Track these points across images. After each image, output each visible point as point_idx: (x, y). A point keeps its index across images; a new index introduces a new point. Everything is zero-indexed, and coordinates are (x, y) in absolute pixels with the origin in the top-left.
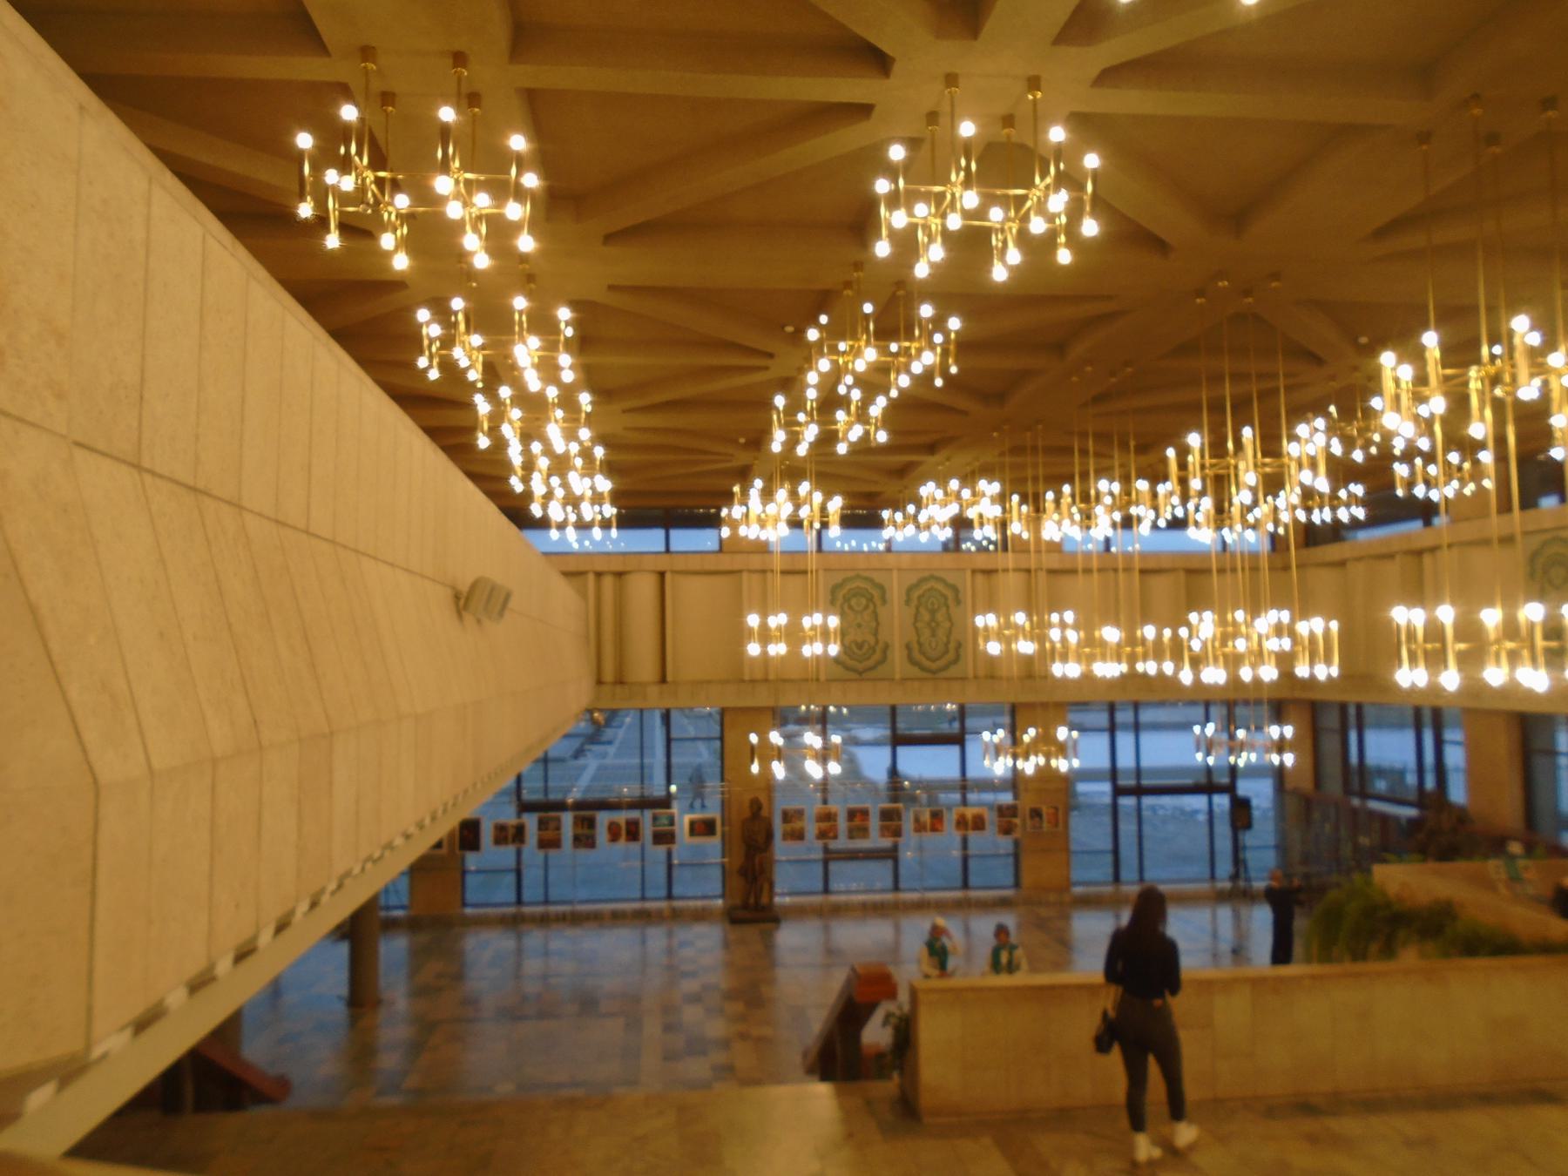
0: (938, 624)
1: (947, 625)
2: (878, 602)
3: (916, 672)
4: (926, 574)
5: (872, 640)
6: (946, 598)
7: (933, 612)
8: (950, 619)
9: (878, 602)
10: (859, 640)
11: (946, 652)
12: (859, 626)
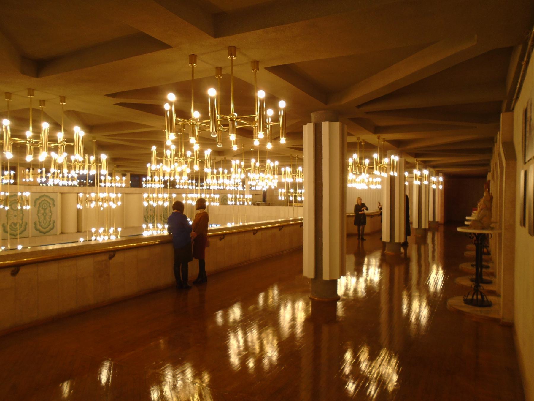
0: (46, 214)
1: (50, 214)
3: (38, 233)
4: (43, 194)
5: (21, 222)
6: (50, 203)
7: (45, 209)
8: (51, 212)
10: (15, 222)
11: (50, 225)
12: (15, 216)
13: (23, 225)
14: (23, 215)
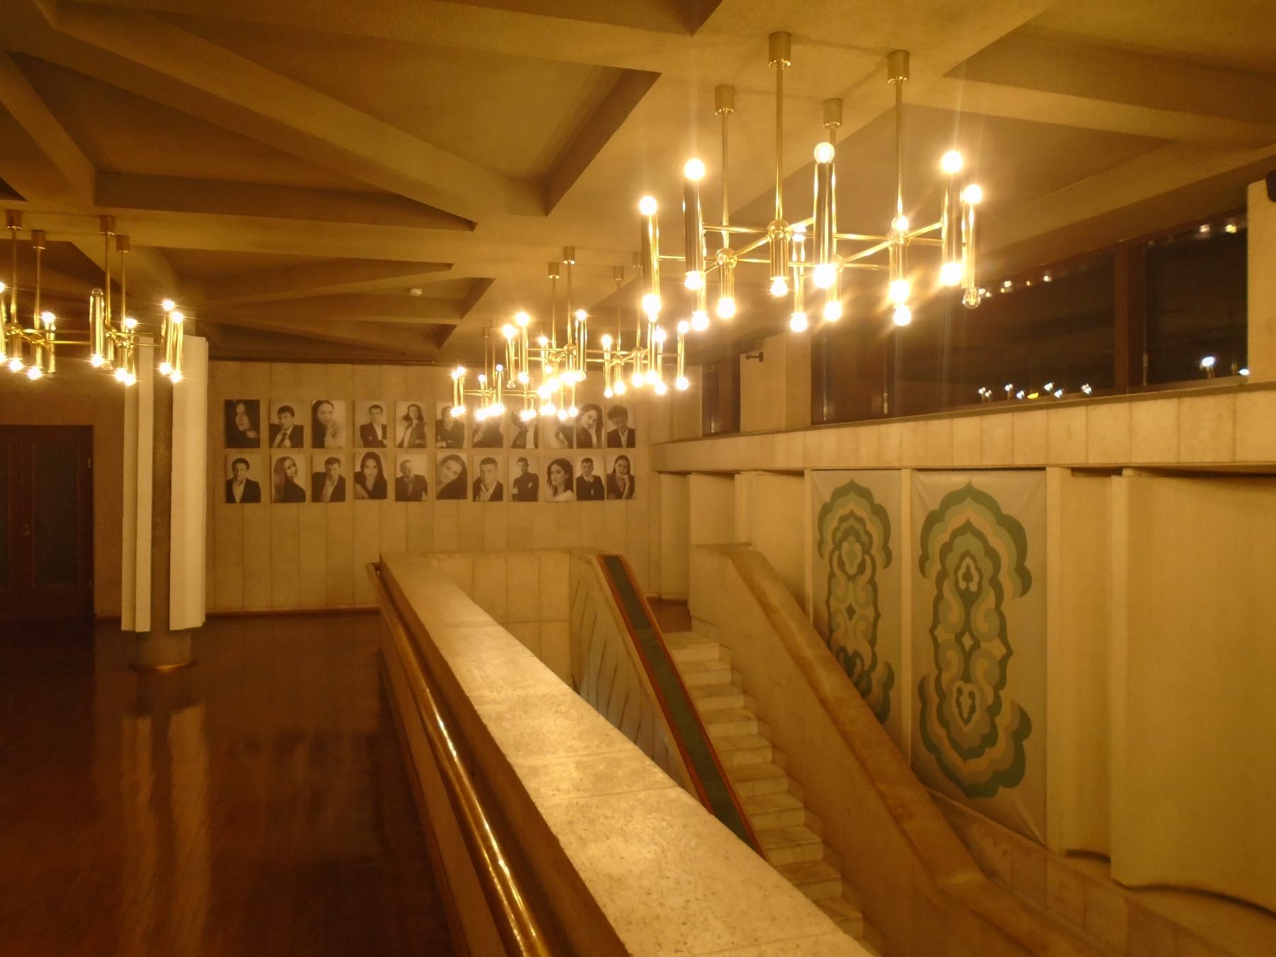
0: (976, 645)
1: (997, 649)
4: (959, 480)
7: (969, 600)
8: (1002, 635)
10: (850, 651)
11: (990, 738)
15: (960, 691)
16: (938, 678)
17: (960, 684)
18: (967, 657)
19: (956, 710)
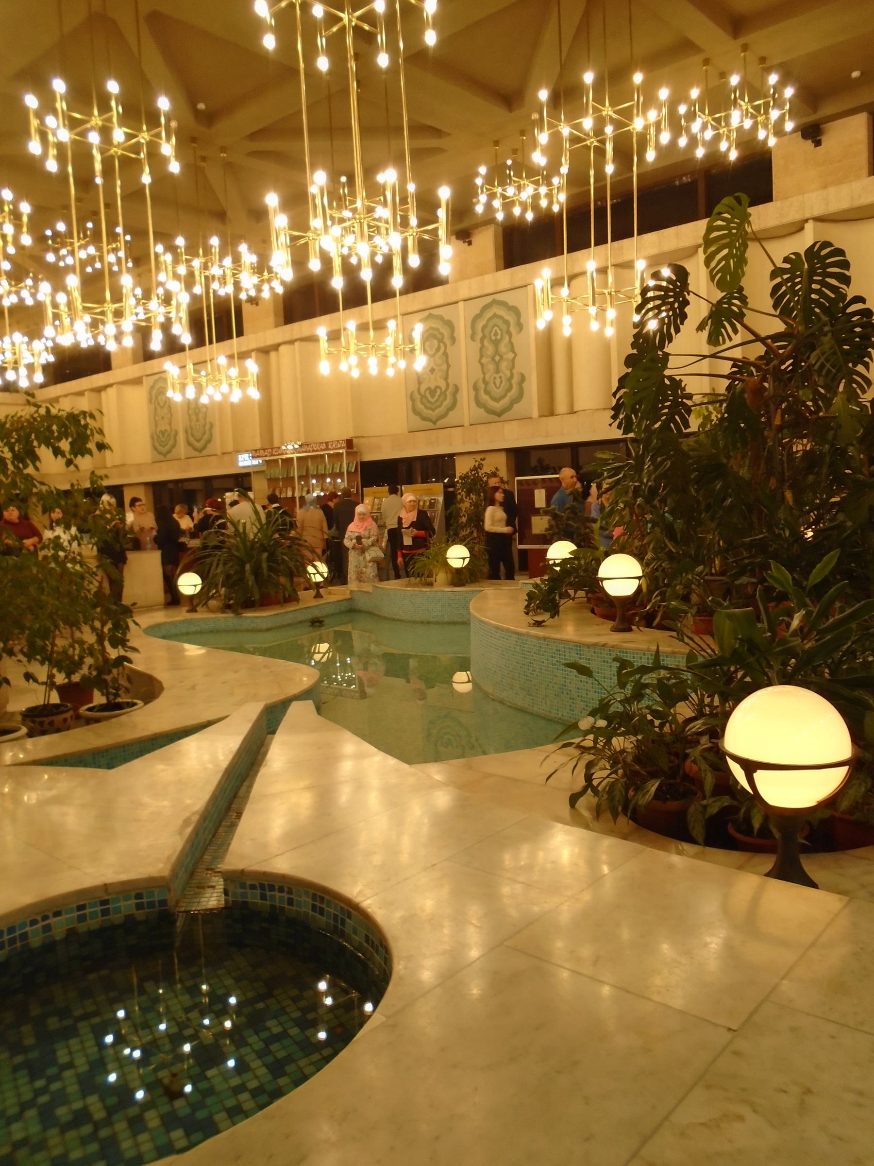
0: (501, 357)
2: (448, 342)
4: (489, 299)
5: (443, 385)
6: (507, 323)
7: (496, 343)
9: (448, 342)
10: (433, 387)
11: (509, 389)
13: (448, 393)
14: (449, 366)
15: (495, 378)
16: (484, 379)
17: (495, 375)
18: (497, 364)
19: (493, 386)
